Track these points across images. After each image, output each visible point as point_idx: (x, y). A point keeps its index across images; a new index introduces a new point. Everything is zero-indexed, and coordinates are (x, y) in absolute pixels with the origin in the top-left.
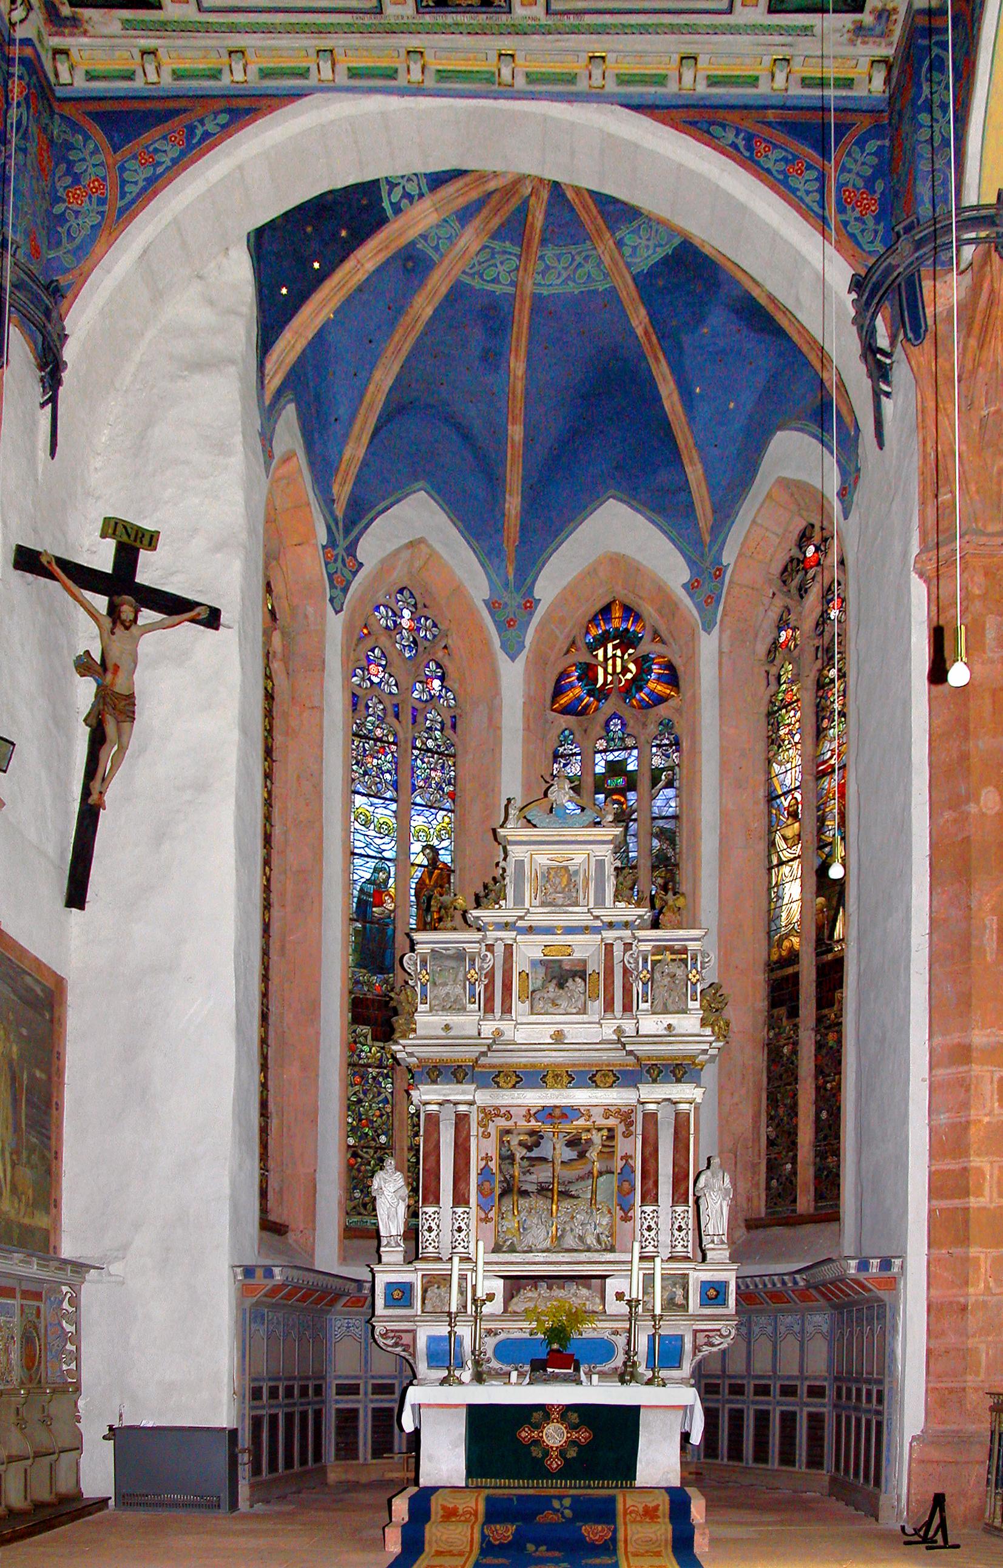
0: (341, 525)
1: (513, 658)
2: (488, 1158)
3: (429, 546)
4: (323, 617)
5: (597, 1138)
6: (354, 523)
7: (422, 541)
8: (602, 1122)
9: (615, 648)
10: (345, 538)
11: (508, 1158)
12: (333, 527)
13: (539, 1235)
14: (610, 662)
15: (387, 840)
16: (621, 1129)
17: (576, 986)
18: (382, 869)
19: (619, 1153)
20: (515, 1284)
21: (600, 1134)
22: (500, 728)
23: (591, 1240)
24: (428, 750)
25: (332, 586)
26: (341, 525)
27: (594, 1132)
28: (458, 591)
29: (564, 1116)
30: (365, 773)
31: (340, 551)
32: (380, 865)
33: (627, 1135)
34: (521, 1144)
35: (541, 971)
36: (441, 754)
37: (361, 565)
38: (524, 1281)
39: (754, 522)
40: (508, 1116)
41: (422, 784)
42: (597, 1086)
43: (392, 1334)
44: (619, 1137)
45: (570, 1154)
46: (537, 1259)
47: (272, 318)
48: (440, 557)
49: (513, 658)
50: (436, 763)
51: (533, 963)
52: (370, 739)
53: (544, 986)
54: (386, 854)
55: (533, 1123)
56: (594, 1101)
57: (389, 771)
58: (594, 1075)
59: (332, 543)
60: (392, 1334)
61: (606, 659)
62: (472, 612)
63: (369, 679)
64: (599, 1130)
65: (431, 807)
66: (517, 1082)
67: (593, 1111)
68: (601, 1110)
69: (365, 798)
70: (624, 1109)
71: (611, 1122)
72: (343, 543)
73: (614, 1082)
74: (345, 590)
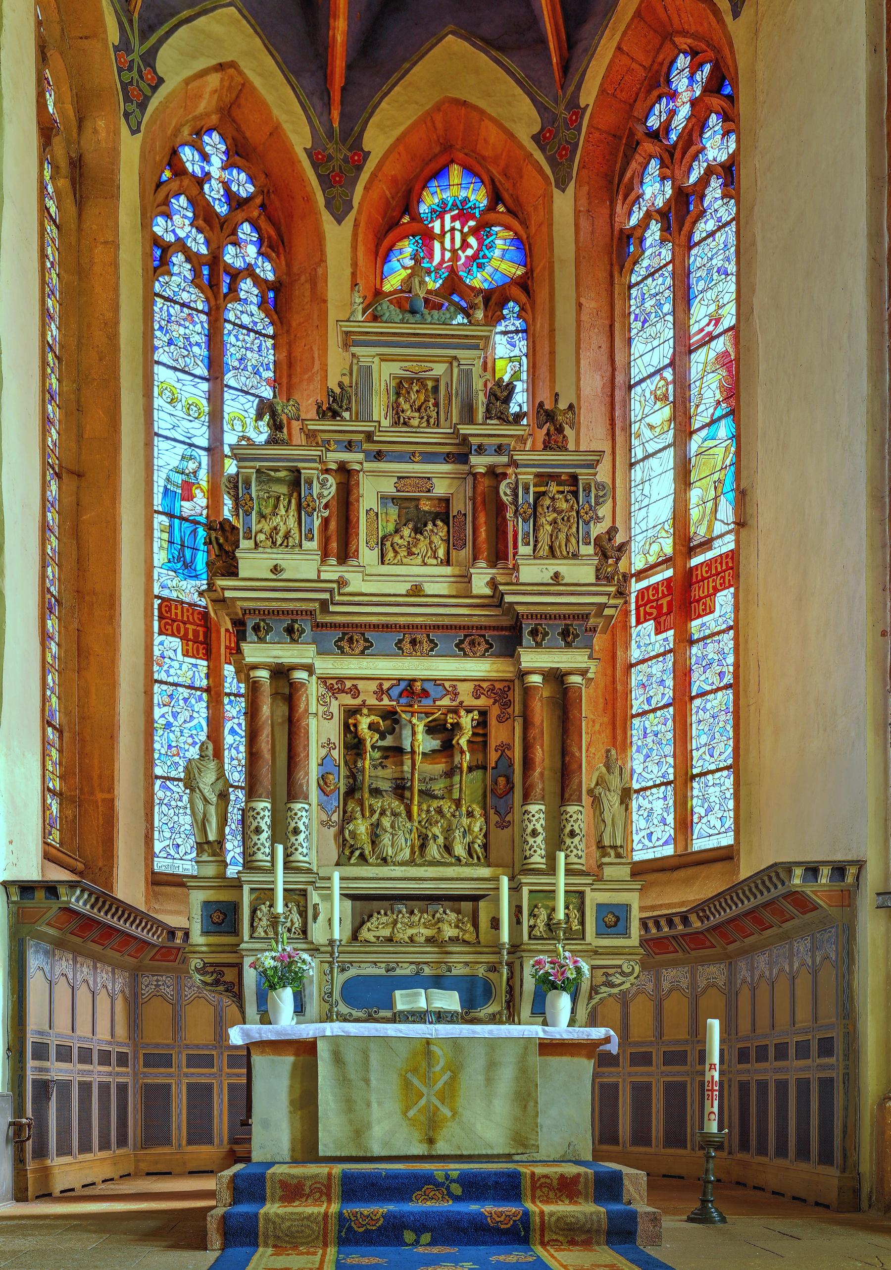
0: (136, 25)
1: (339, 222)
3: (241, 73)
4: (117, 133)
5: (467, 721)
6: (152, 29)
7: (233, 65)
8: (470, 701)
9: (453, 219)
10: (141, 44)
12: (127, 25)
13: (398, 842)
14: (448, 236)
15: (196, 424)
16: (495, 711)
17: (438, 533)
18: (191, 458)
20: (365, 904)
21: (470, 715)
22: (325, 301)
24: (242, 326)
25: (127, 99)
26: (136, 25)
27: (463, 713)
28: (276, 131)
29: (425, 693)
30: (170, 343)
31: (135, 56)
32: (189, 452)
34: (372, 727)
35: (393, 511)
36: (256, 332)
37: (161, 81)
38: (376, 904)
39: (619, 48)
40: (355, 692)
41: (236, 364)
42: (466, 655)
44: (493, 721)
48: (253, 89)
49: (339, 222)
50: (253, 343)
51: (384, 499)
52: (176, 302)
53: (397, 531)
54: (195, 441)
55: (386, 701)
56: (462, 674)
57: (198, 344)
58: (462, 642)
59: (124, 46)
61: (443, 233)
62: (293, 161)
63: (173, 231)
64: (469, 711)
65: (247, 393)
66: (366, 648)
67: (462, 687)
68: (470, 686)
69: (171, 372)
71: (482, 702)
72: (139, 49)
73: (487, 650)
74: (143, 106)
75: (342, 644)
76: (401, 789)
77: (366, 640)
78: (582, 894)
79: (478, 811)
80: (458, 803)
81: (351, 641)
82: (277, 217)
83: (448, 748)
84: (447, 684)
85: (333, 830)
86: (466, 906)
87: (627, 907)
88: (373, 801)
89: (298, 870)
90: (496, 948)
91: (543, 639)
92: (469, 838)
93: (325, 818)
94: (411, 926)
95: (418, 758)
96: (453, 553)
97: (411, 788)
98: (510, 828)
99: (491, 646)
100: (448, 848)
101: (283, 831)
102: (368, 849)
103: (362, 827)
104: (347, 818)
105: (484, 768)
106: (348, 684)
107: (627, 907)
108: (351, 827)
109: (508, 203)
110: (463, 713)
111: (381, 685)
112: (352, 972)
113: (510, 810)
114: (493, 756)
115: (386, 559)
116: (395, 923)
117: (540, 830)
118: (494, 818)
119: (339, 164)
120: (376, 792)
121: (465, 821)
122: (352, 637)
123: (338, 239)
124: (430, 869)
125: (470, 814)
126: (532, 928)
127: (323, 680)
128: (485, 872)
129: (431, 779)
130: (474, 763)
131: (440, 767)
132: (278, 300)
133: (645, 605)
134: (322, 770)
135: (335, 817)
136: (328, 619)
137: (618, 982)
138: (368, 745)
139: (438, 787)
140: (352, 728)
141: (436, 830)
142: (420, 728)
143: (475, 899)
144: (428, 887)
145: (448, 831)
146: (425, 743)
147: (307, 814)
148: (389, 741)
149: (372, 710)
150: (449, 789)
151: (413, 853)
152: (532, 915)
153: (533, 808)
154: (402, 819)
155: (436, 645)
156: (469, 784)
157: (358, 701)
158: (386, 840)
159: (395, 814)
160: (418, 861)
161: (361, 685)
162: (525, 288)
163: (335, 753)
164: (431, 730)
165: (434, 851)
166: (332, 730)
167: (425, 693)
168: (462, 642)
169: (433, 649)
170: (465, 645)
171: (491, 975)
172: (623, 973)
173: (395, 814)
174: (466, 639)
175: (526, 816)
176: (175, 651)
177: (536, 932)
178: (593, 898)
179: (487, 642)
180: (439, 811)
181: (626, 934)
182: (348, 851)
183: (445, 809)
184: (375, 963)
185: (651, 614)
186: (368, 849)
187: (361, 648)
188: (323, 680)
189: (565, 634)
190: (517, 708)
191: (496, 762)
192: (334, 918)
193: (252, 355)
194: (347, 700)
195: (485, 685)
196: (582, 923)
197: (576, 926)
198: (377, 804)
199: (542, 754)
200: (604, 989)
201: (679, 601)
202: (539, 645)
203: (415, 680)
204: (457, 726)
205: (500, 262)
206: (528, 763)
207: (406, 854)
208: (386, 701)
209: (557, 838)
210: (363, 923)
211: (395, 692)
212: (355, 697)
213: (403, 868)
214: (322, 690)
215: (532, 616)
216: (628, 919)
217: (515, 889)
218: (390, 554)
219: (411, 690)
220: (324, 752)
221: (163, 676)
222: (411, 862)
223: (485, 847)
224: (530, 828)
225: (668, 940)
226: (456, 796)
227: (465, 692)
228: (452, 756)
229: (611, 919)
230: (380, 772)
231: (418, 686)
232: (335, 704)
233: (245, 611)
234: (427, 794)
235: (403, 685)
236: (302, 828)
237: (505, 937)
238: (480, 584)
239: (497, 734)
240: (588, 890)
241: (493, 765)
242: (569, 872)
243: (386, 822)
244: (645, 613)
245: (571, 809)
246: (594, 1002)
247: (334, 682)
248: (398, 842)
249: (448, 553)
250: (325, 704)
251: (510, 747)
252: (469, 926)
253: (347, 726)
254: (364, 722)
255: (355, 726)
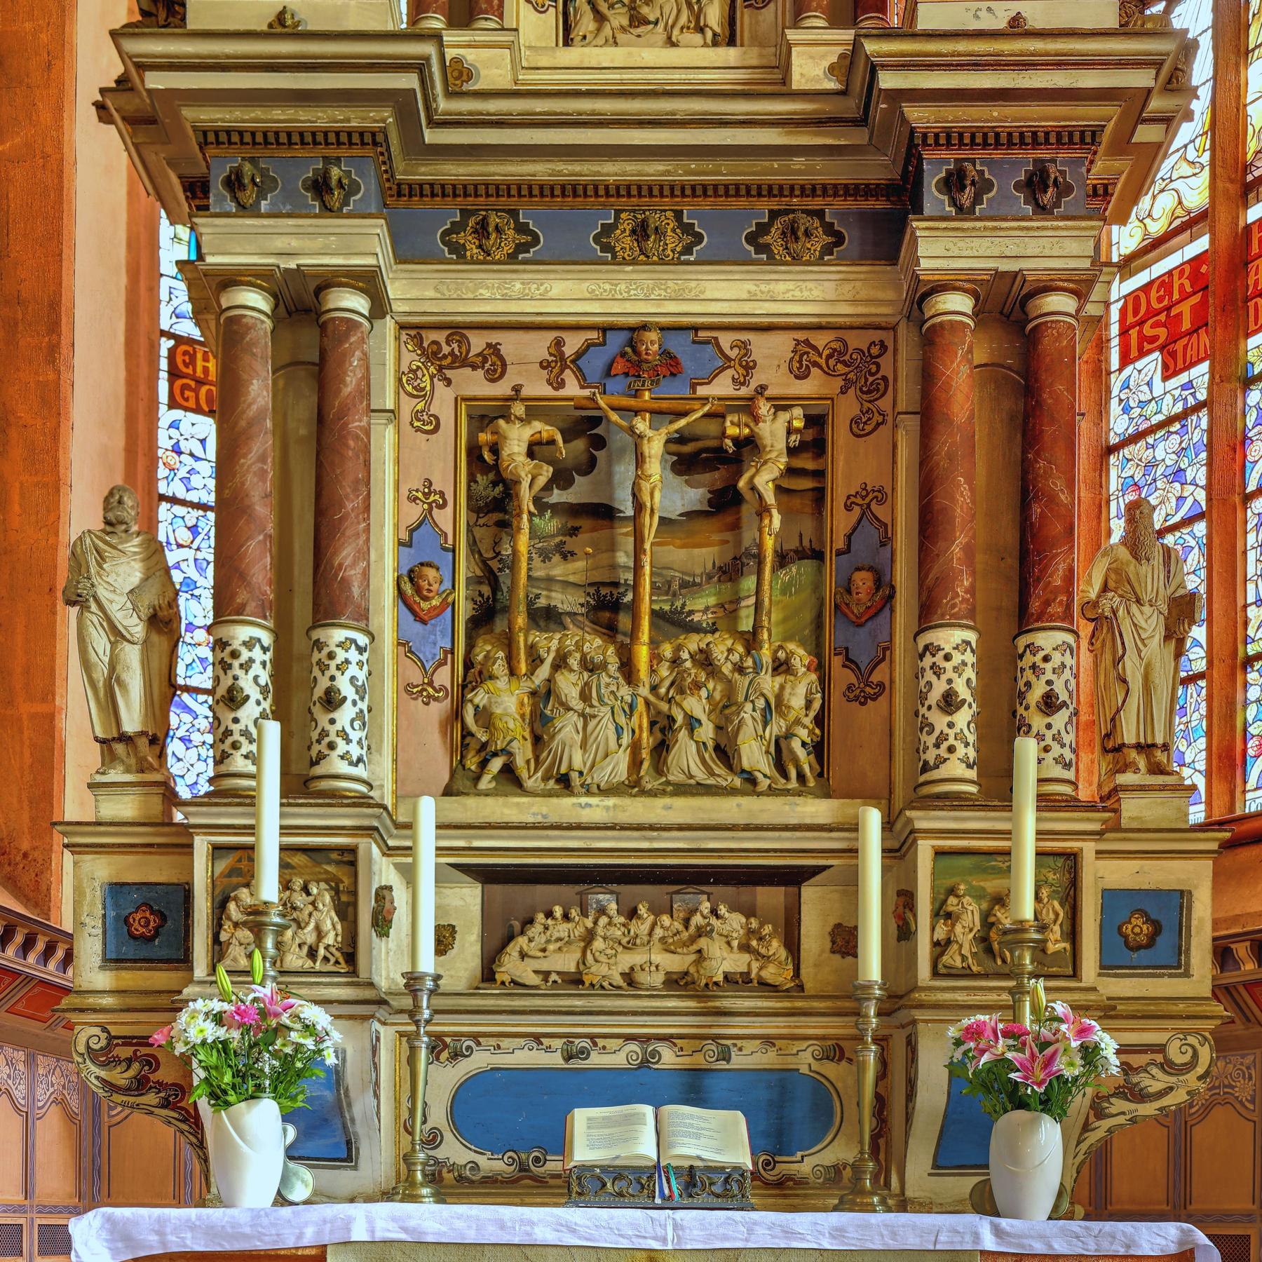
2: (428, 495)
5: (775, 432)
11: (494, 503)
13: (598, 738)
19: (841, 486)
20: (514, 888)
21: (784, 417)
23: (754, 754)
29: (671, 365)
33: (859, 428)
38: (542, 892)
40: (494, 363)
42: (772, 261)
43: (126, 1052)
44: (840, 436)
45: (687, 496)
46: (587, 816)
55: (572, 388)
58: (763, 229)
60: (126, 1052)
66: (522, 248)
68: (782, 344)
70: (857, 341)
73: (827, 250)
75: (461, 238)
76: (607, 609)
77: (522, 229)
78: (1072, 859)
79: (801, 657)
80: (751, 641)
81: (482, 230)
83: (726, 503)
84: (726, 339)
85: (439, 709)
86: (771, 897)
87: (1181, 899)
88: (536, 637)
89: (335, 798)
90: (848, 997)
91: (977, 200)
92: (777, 727)
93: (416, 677)
94: (631, 946)
95: (650, 526)
96: (745, 18)
97: (633, 609)
98: (883, 700)
99: (839, 239)
100: (725, 753)
101: (300, 697)
102: (523, 753)
103: (507, 699)
104: (473, 675)
105: (818, 555)
106: (478, 342)
107: (1181, 899)
108: (480, 698)
110: (764, 408)
111: (559, 343)
112: (480, 1060)
113: (884, 653)
114: (840, 522)
115: (576, 34)
116: (589, 936)
117: (964, 692)
118: (842, 676)
120: (546, 618)
121: (769, 683)
122: (483, 217)
124: (680, 802)
125: (782, 667)
126: (941, 947)
127: (412, 330)
128: (817, 809)
129: (684, 585)
130: (793, 544)
131: (702, 556)
133: (1141, 323)
134: (411, 558)
135: (443, 677)
136: (427, 172)
137: (1156, 1087)
138: (526, 495)
139: (701, 605)
140: (487, 456)
141: (696, 705)
142: (655, 446)
143: (793, 877)
144: (672, 848)
145: (725, 710)
146: (668, 494)
147: (364, 661)
148: (580, 491)
149: (536, 410)
150: (730, 610)
151: (636, 763)
152: (941, 913)
153: (950, 638)
154: (610, 680)
155: (699, 238)
156: (775, 595)
157: (502, 389)
158: (567, 729)
159: (590, 667)
160: (650, 783)
161: (510, 344)
163: (444, 518)
164: (688, 459)
165: (687, 756)
166: (441, 462)
167: (671, 365)
168: (763, 229)
169: (692, 249)
170: (773, 237)
171: (831, 1070)
172: (1168, 1066)
173: (590, 667)
174: (775, 221)
175: (928, 660)
176: (203, 441)
177: (952, 959)
178: (1102, 873)
179: (829, 229)
180: (705, 660)
181: (1177, 964)
182: (474, 758)
183: (719, 653)
184: (537, 1038)
185: (1154, 339)
186: (523, 753)
187: (508, 249)
188: (412, 330)
189: (1036, 184)
190: (906, 393)
191: (849, 537)
192: (424, 917)
194: (475, 384)
195: (821, 340)
196: (1073, 934)
197: (1056, 943)
198: (548, 643)
199: (970, 497)
200: (1118, 1105)
202: (964, 212)
203: (644, 327)
204: (750, 445)
206: (930, 523)
207: (619, 767)
208: (572, 388)
209: (1002, 726)
210: (510, 938)
211: (595, 363)
212: (495, 376)
213: (611, 802)
214: (411, 358)
215: (948, 139)
216: (1182, 929)
217: (898, 851)
218: (586, 23)
219: (631, 354)
220: (414, 513)
221: (178, 490)
222: (632, 787)
223: (818, 749)
224: (939, 688)
226: (746, 624)
227: (772, 354)
228: (736, 526)
229: (1138, 928)
230: (559, 569)
231: (652, 342)
232: (443, 403)
233: (210, 138)
234: (673, 622)
235: (616, 341)
236: (347, 690)
237: (872, 966)
238: (813, 62)
239: (849, 465)
240: (1088, 848)
241: (840, 544)
242: (1046, 803)
243: (569, 686)
244: (1142, 338)
245: (1048, 640)
246: (1093, 1137)
247: (440, 336)
248: (598, 738)
249: (731, 21)
250: (419, 394)
251: (881, 495)
252: (776, 947)
253: (474, 453)
254: (516, 439)
255: (495, 449)
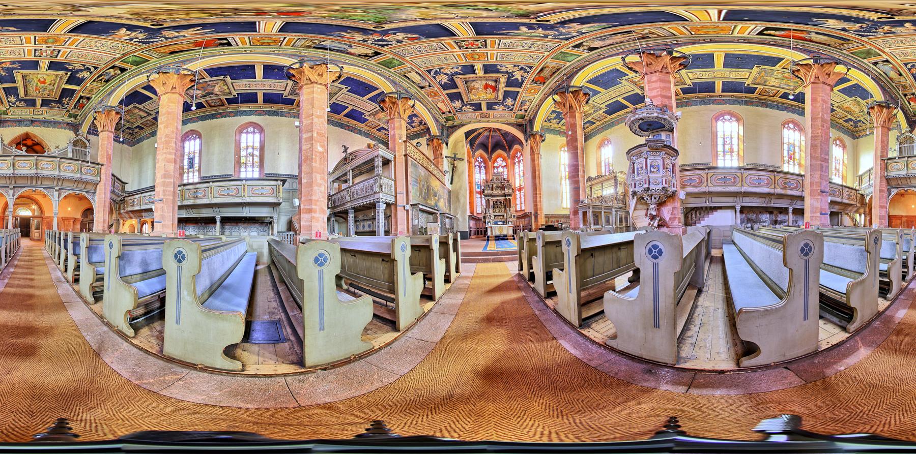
47: (467, 138)
82: (485, 161)
109: (504, 160)
119: (490, 158)
123: (490, 163)
132: (485, 167)
162: (506, 166)
193: (483, 171)
201: (520, 190)
205: (504, 164)
225: (519, 218)
